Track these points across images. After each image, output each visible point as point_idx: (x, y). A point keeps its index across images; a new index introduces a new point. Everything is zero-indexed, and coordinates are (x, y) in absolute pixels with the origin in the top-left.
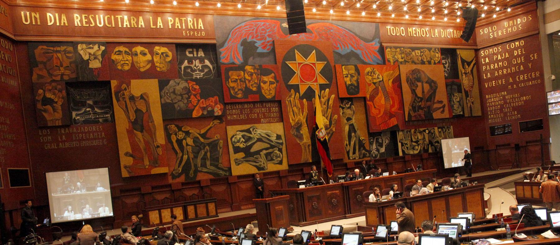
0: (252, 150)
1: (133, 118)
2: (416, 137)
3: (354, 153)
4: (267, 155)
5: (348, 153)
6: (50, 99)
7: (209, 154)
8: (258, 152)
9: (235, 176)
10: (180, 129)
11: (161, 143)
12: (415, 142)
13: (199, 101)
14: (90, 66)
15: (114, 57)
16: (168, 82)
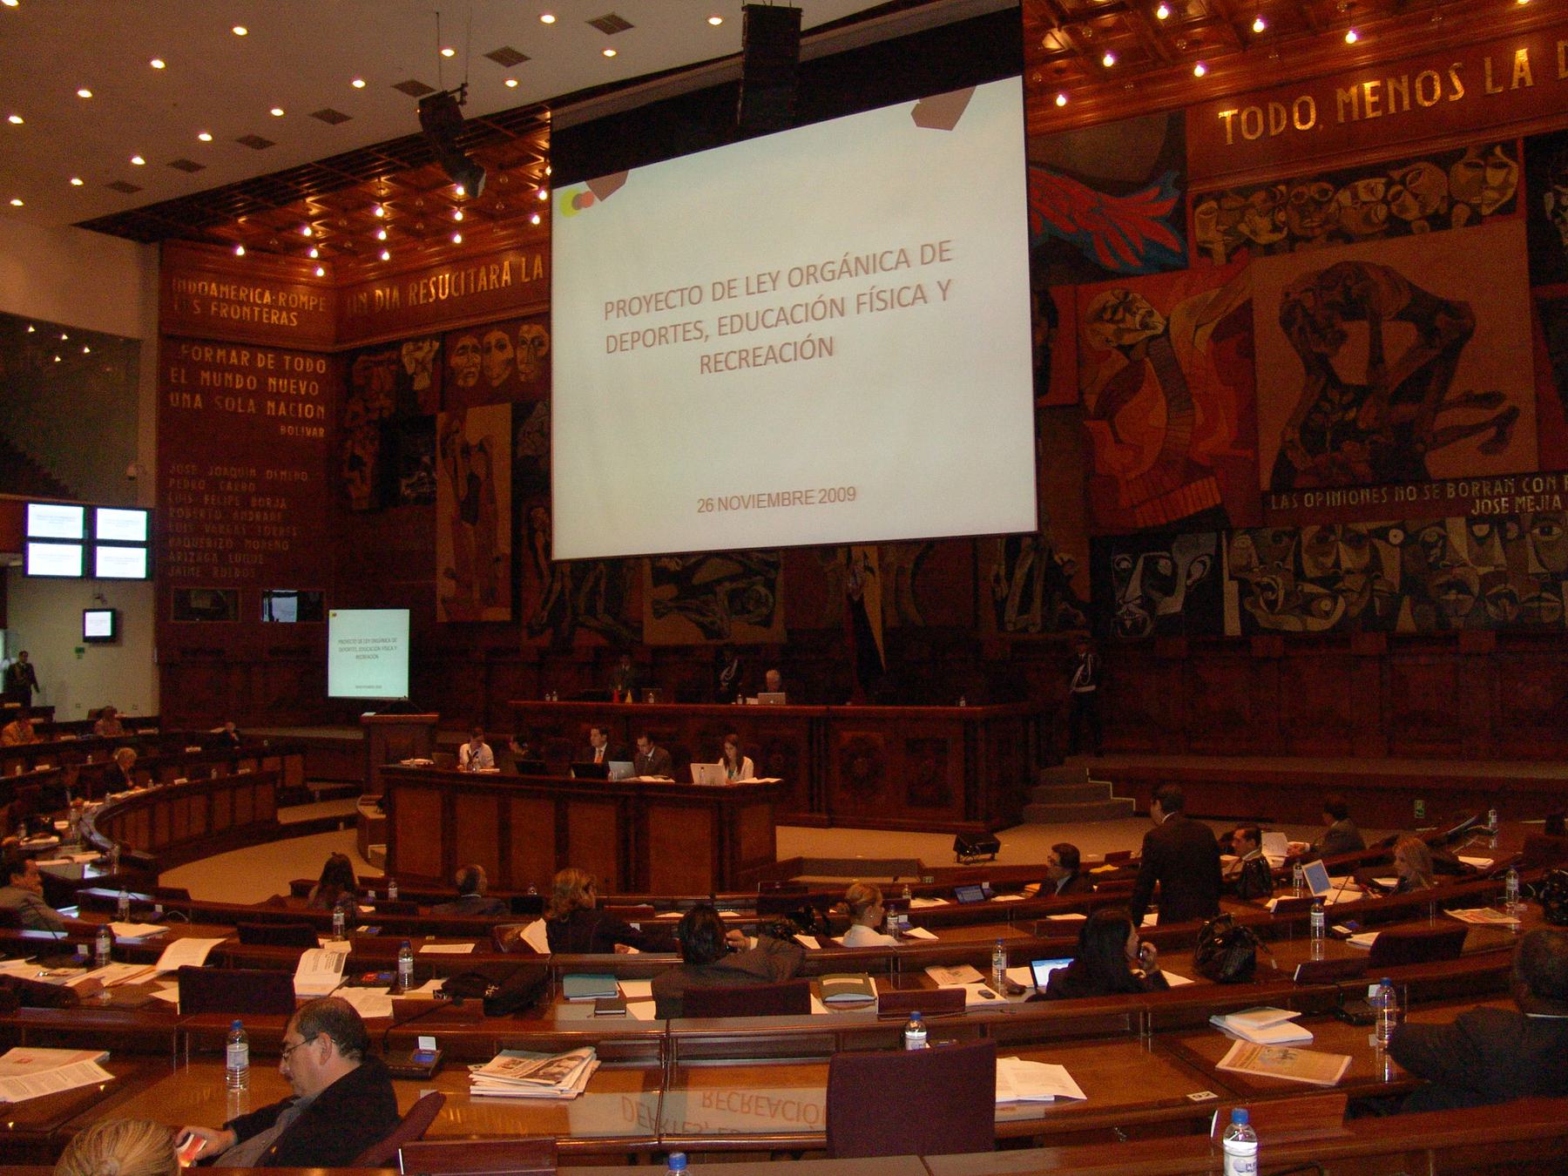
0: (695, 581)
1: (463, 493)
2: (1329, 561)
3: (1025, 607)
4: (733, 596)
5: (1000, 606)
7: (603, 581)
8: (709, 587)
12: (1312, 581)
15: (457, 361)
16: (533, 406)
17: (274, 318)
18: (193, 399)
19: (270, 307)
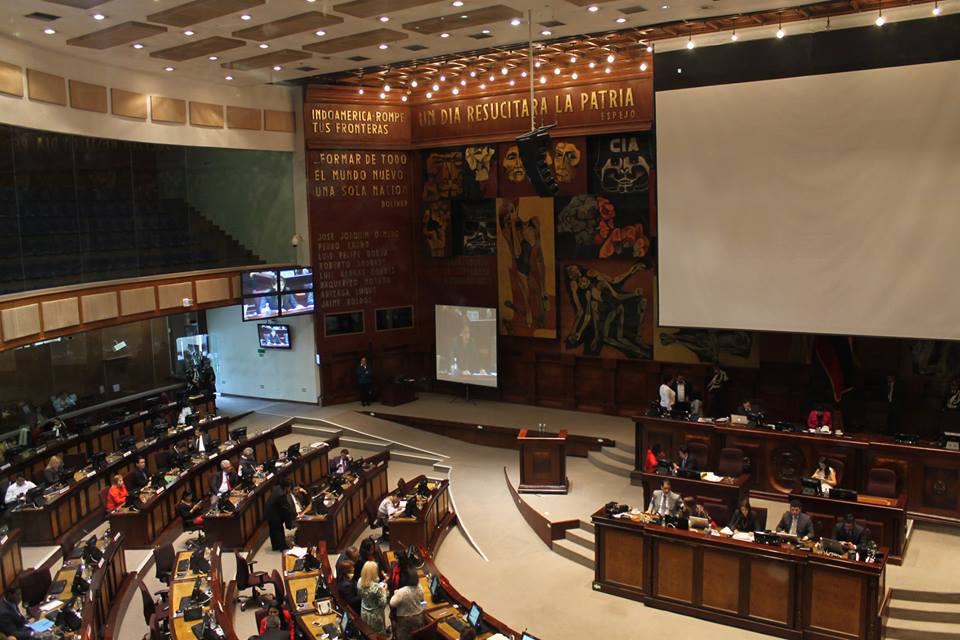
1: (517, 254)
6: (435, 222)
9: (657, 363)
10: (584, 274)
11: (550, 293)
13: (611, 230)
14: (477, 179)
15: (507, 163)
16: (567, 199)
17: (374, 130)
18: (329, 189)
19: (371, 122)
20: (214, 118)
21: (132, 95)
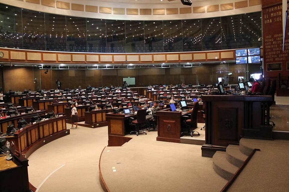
20: (230, 7)
21: (200, 7)
